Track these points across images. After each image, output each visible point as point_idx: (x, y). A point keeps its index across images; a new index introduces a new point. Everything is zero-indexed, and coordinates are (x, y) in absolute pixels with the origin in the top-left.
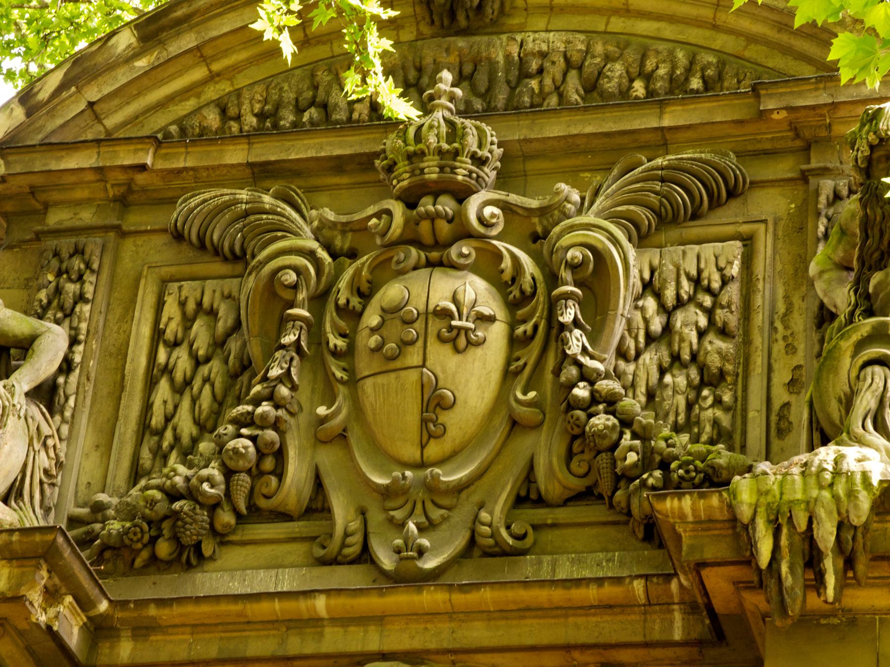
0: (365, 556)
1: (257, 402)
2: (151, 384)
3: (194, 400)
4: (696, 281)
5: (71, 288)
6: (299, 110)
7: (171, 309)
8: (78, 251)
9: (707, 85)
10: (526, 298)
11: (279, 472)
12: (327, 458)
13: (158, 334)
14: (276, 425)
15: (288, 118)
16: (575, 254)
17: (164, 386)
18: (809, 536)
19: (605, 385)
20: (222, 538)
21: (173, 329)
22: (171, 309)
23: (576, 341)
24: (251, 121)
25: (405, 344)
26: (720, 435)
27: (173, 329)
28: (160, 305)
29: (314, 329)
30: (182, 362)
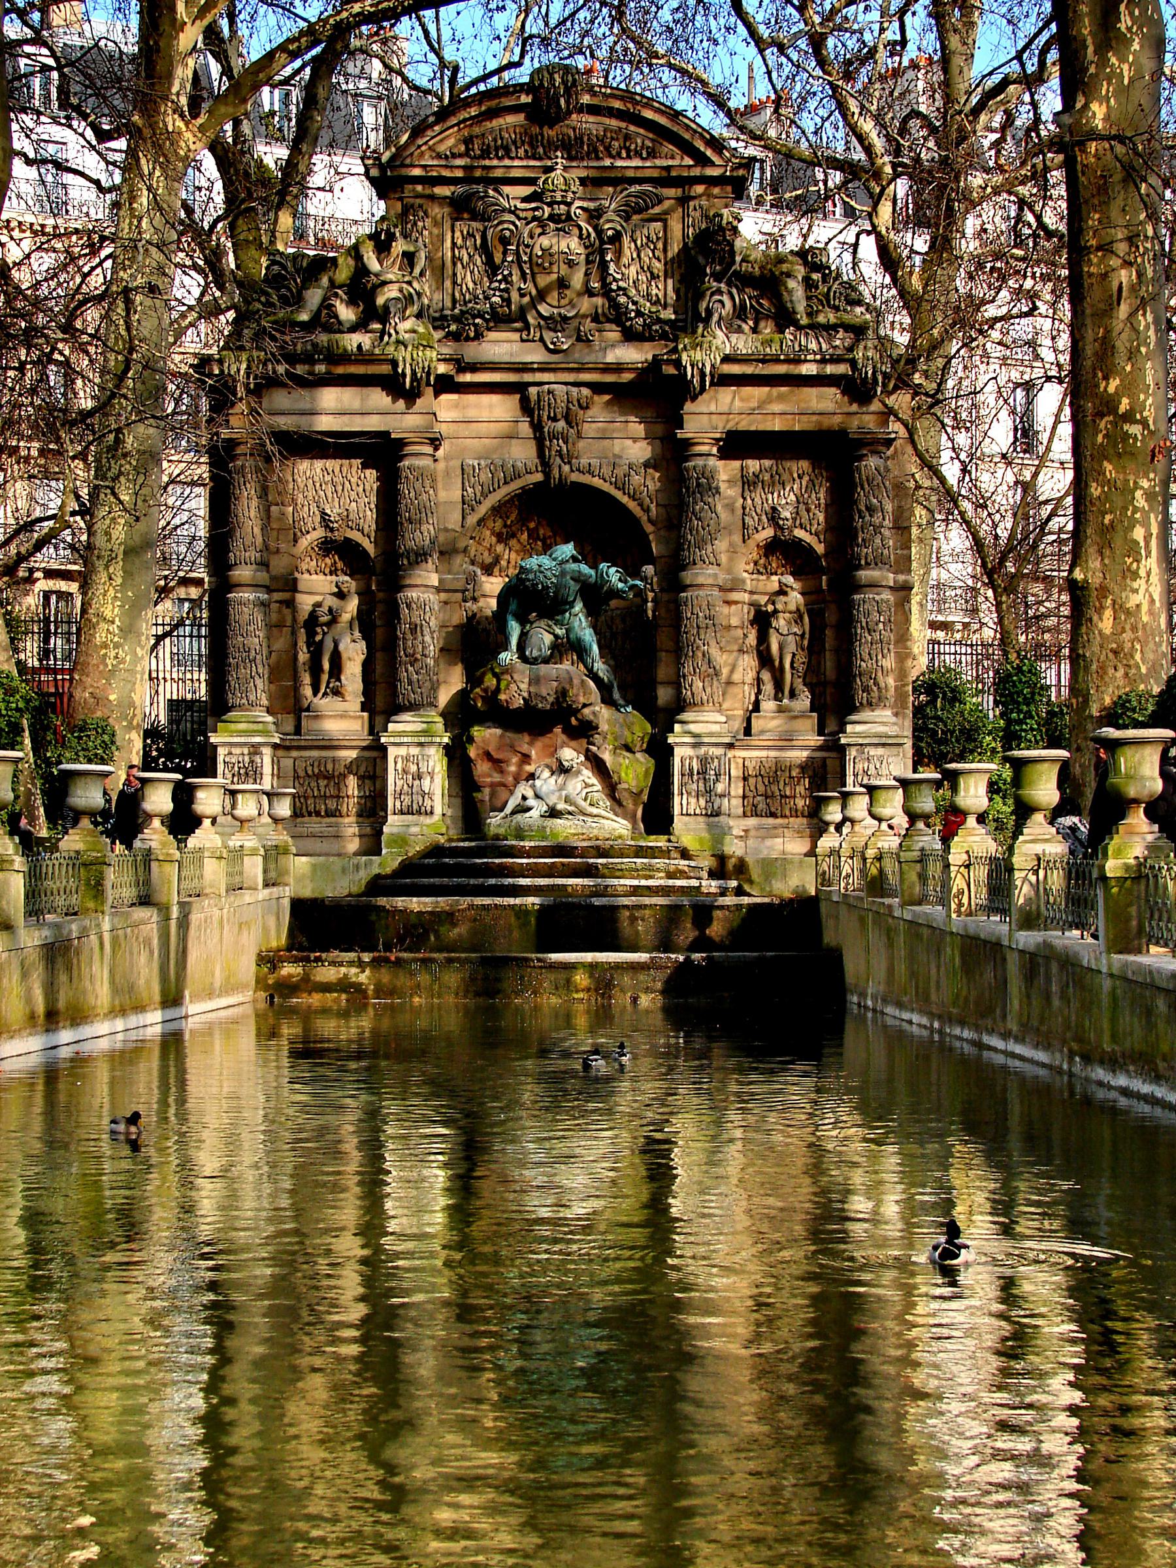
1: (500, 282)
2: (454, 264)
3: (472, 272)
4: (648, 238)
5: (420, 224)
6: (497, 149)
7: (458, 234)
8: (421, 206)
9: (649, 154)
13: (454, 244)
14: (506, 290)
16: (610, 233)
17: (459, 265)
19: (621, 284)
20: (489, 329)
21: (459, 242)
22: (458, 234)
23: (612, 266)
26: (658, 302)
27: (459, 242)
28: (453, 232)
29: (517, 253)
30: (466, 258)
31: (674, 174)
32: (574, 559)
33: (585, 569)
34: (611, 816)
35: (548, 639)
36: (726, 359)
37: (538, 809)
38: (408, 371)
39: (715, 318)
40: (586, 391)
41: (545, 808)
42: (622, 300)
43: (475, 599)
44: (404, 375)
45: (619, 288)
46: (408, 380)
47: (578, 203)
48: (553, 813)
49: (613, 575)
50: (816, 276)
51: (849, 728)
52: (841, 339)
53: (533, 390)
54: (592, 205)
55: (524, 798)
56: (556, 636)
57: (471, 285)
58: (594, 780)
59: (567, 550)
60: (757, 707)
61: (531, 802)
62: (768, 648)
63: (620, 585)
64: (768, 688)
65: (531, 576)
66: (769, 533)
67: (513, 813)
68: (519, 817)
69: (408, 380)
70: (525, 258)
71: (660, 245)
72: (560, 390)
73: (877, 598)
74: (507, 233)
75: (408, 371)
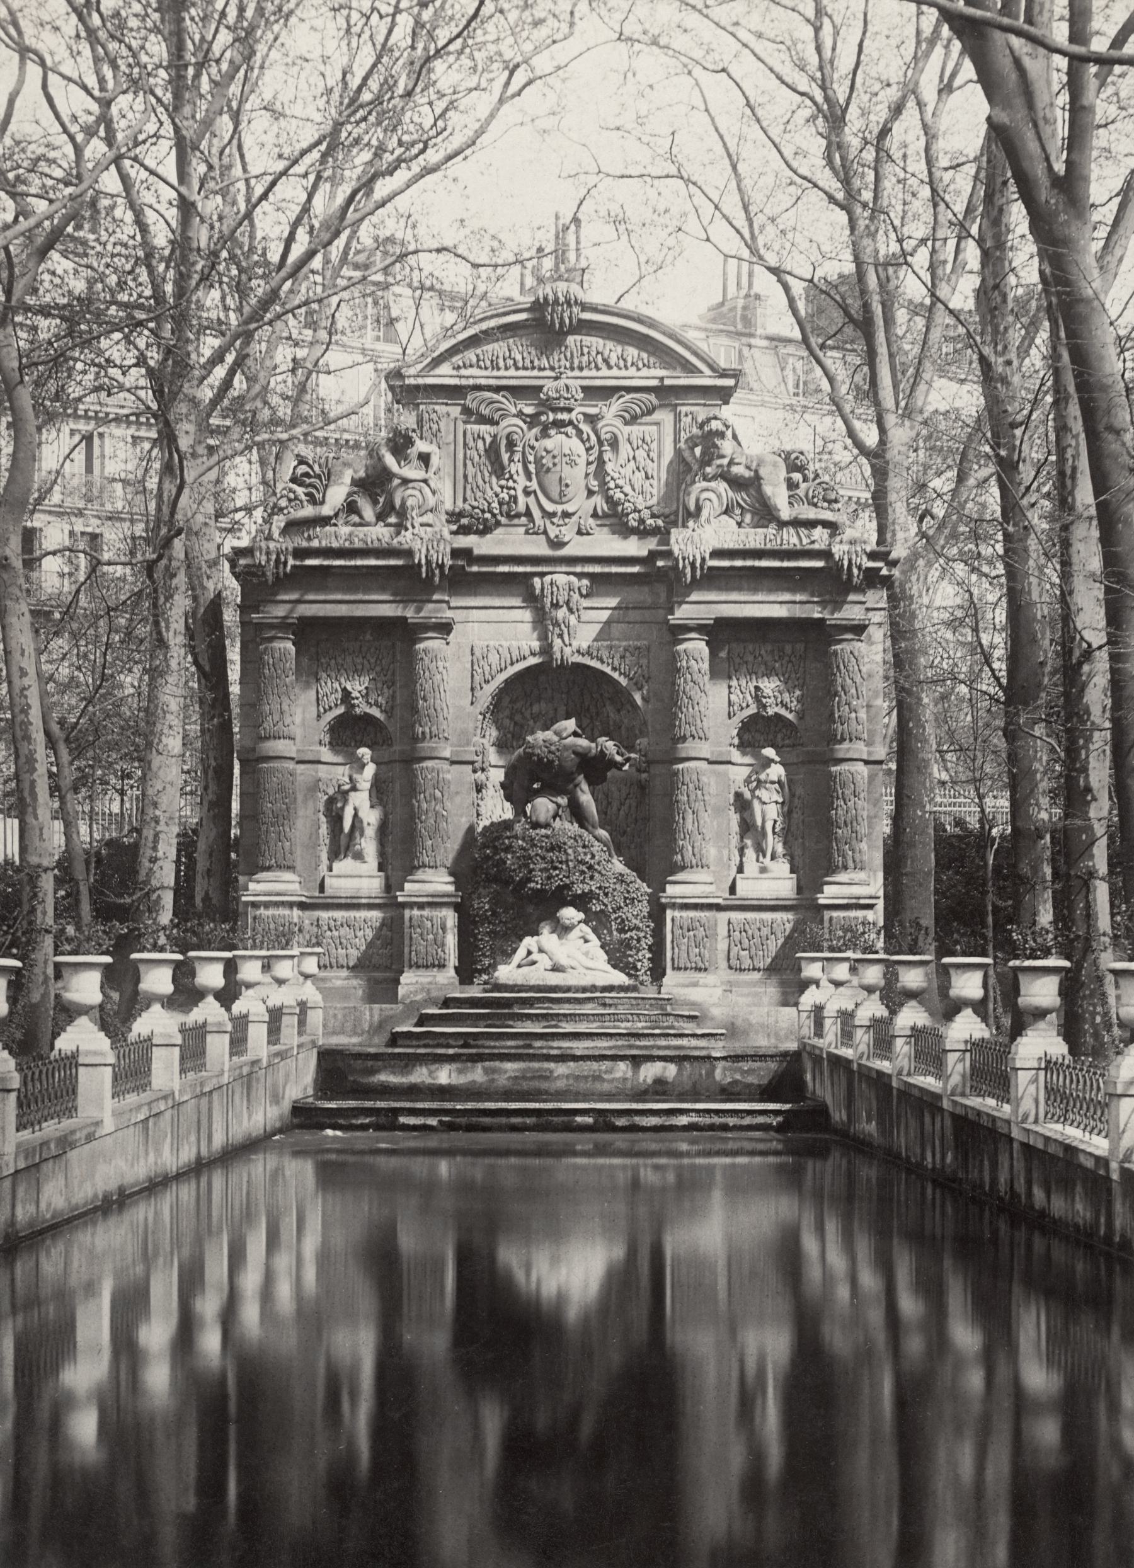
0: (545, 532)
10: (591, 448)
11: (516, 502)
12: (531, 500)
13: (465, 445)
15: (501, 363)
16: (608, 436)
18: (693, 565)
19: (620, 482)
20: (498, 524)
21: (471, 444)
24: (488, 363)
25: (555, 465)
31: (667, 382)
32: (575, 734)
33: (583, 742)
34: (609, 968)
35: (552, 807)
36: (717, 554)
37: (544, 961)
38: (423, 561)
39: (705, 513)
40: (585, 582)
41: (548, 964)
42: (618, 495)
43: (483, 770)
44: (420, 565)
45: (617, 486)
46: (424, 570)
47: (579, 409)
48: (556, 968)
49: (610, 746)
50: (797, 476)
51: (827, 889)
52: (819, 533)
53: (537, 581)
54: (592, 411)
55: (529, 953)
56: (559, 806)
57: (480, 482)
58: (592, 937)
59: (571, 724)
60: (740, 870)
61: (534, 957)
62: (752, 815)
63: (618, 758)
64: (750, 853)
65: (538, 751)
66: (753, 710)
67: (519, 966)
68: (525, 969)
69: (424, 570)
70: (531, 458)
71: (654, 446)
72: (561, 579)
73: (852, 769)
74: (515, 437)
75: (423, 561)
